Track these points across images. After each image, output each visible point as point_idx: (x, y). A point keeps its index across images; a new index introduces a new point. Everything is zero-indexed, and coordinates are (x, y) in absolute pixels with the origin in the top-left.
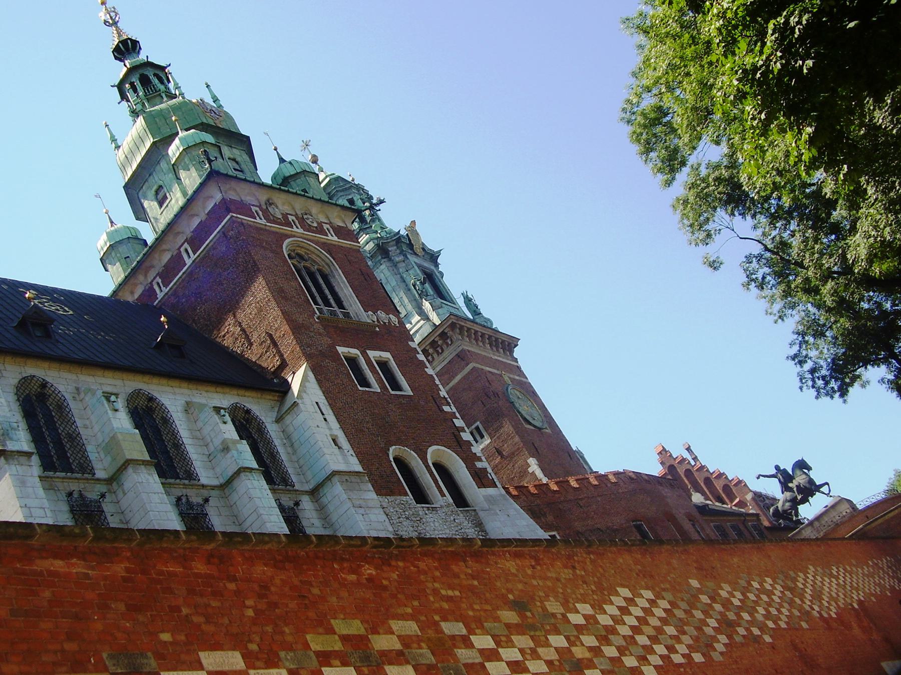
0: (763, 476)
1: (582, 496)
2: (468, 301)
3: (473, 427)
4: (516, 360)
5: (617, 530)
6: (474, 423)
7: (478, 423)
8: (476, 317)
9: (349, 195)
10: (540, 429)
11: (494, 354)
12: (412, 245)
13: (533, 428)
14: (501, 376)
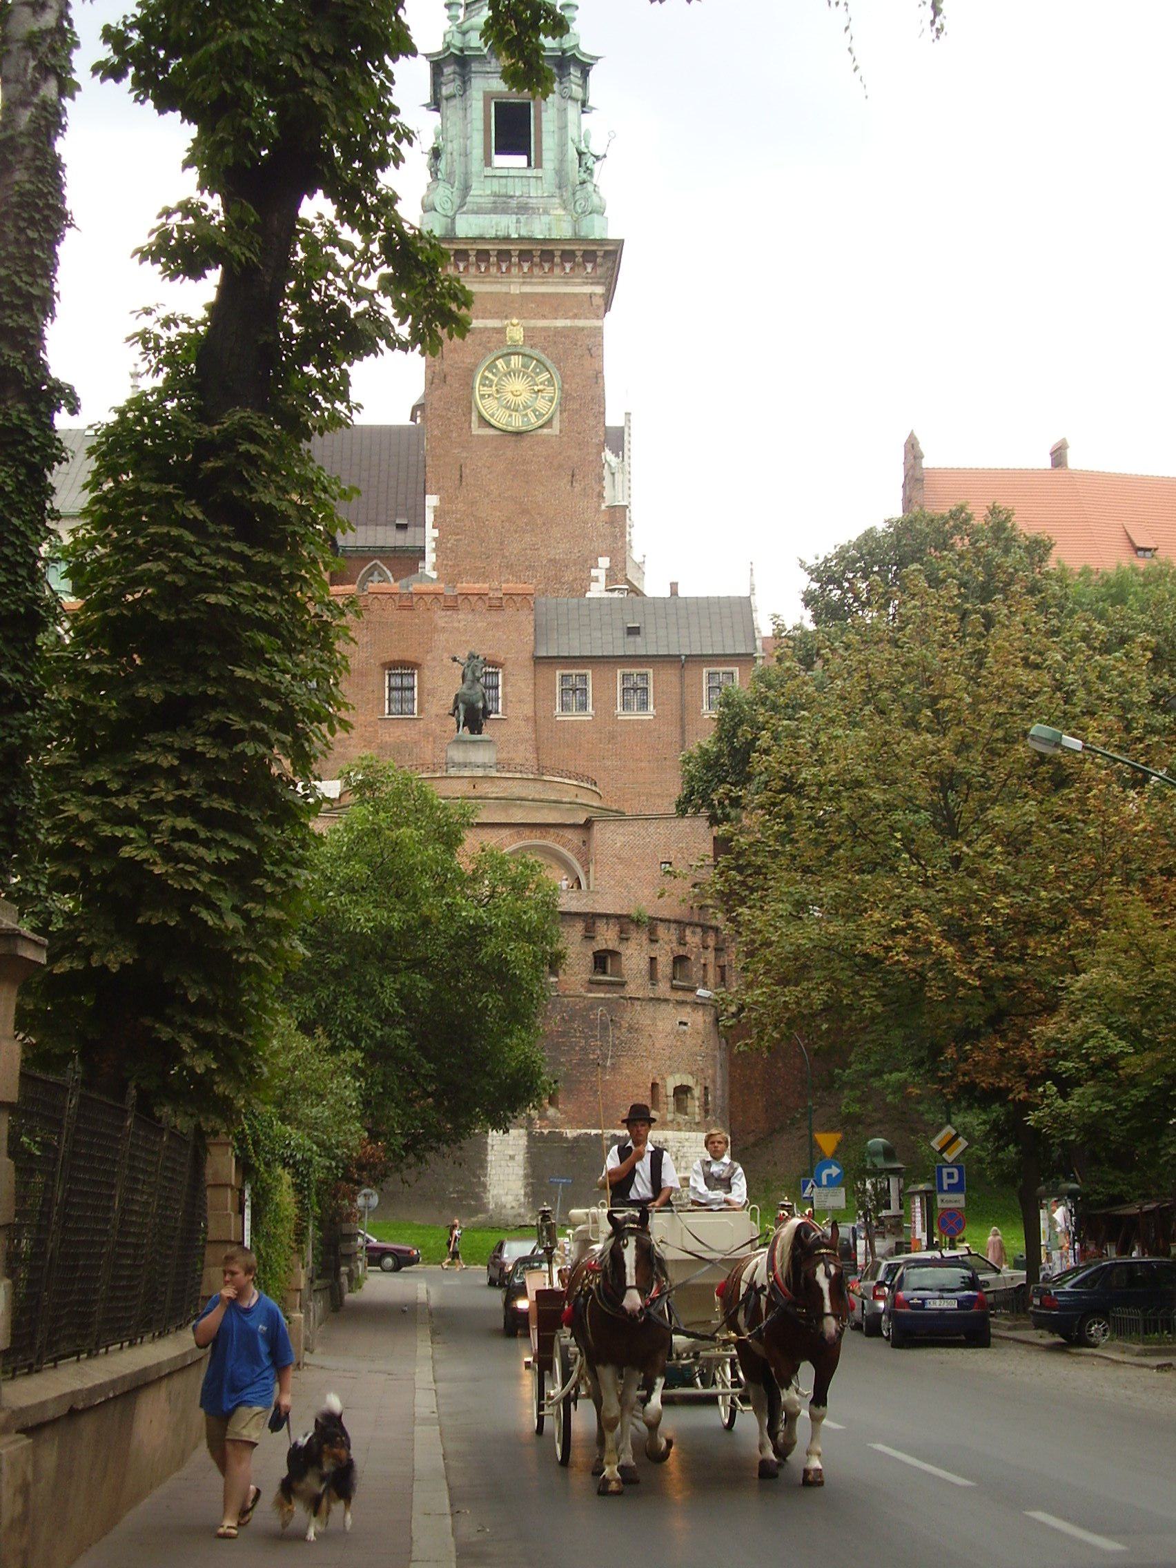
10: (518, 434)
14: (501, 331)
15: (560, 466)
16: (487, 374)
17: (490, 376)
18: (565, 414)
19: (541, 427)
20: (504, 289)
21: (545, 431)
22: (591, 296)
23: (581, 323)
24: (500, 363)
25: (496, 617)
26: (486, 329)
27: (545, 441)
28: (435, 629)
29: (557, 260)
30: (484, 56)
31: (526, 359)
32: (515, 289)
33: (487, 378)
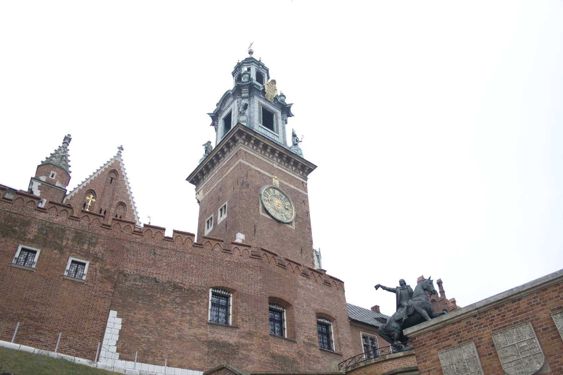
0: (384, 288)
1: (169, 247)
2: (294, 136)
3: (224, 205)
4: (306, 179)
5: (181, 288)
6: (225, 202)
7: (227, 202)
8: (293, 146)
9: (250, 65)
10: (279, 222)
11: (279, 165)
12: (265, 93)
13: (272, 219)
14: (271, 178)
15: (296, 244)
16: (266, 191)
17: (267, 193)
18: (297, 223)
19: (288, 223)
20: (271, 164)
21: (290, 226)
22: (303, 182)
23: (300, 191)
24: (271, 190)
25: (327, 290)
26: (264, 175)
27: (290, 230)
28: (298, 286)
29: (292, 163)
30: (260, 91)
31: (281, 194)
32: (275, 166)
33: (266, 193)
